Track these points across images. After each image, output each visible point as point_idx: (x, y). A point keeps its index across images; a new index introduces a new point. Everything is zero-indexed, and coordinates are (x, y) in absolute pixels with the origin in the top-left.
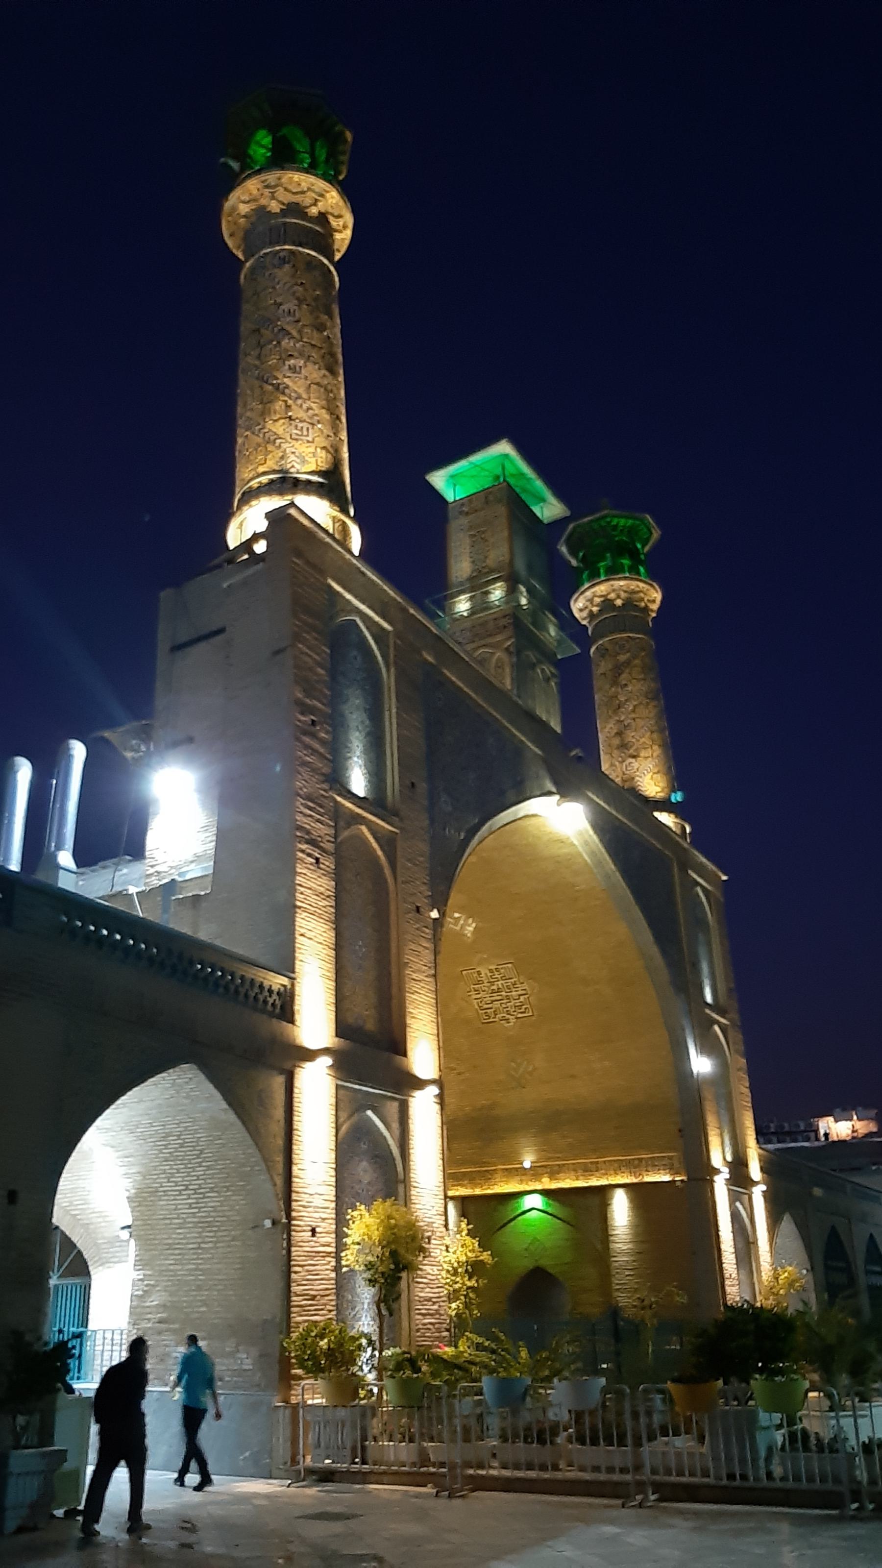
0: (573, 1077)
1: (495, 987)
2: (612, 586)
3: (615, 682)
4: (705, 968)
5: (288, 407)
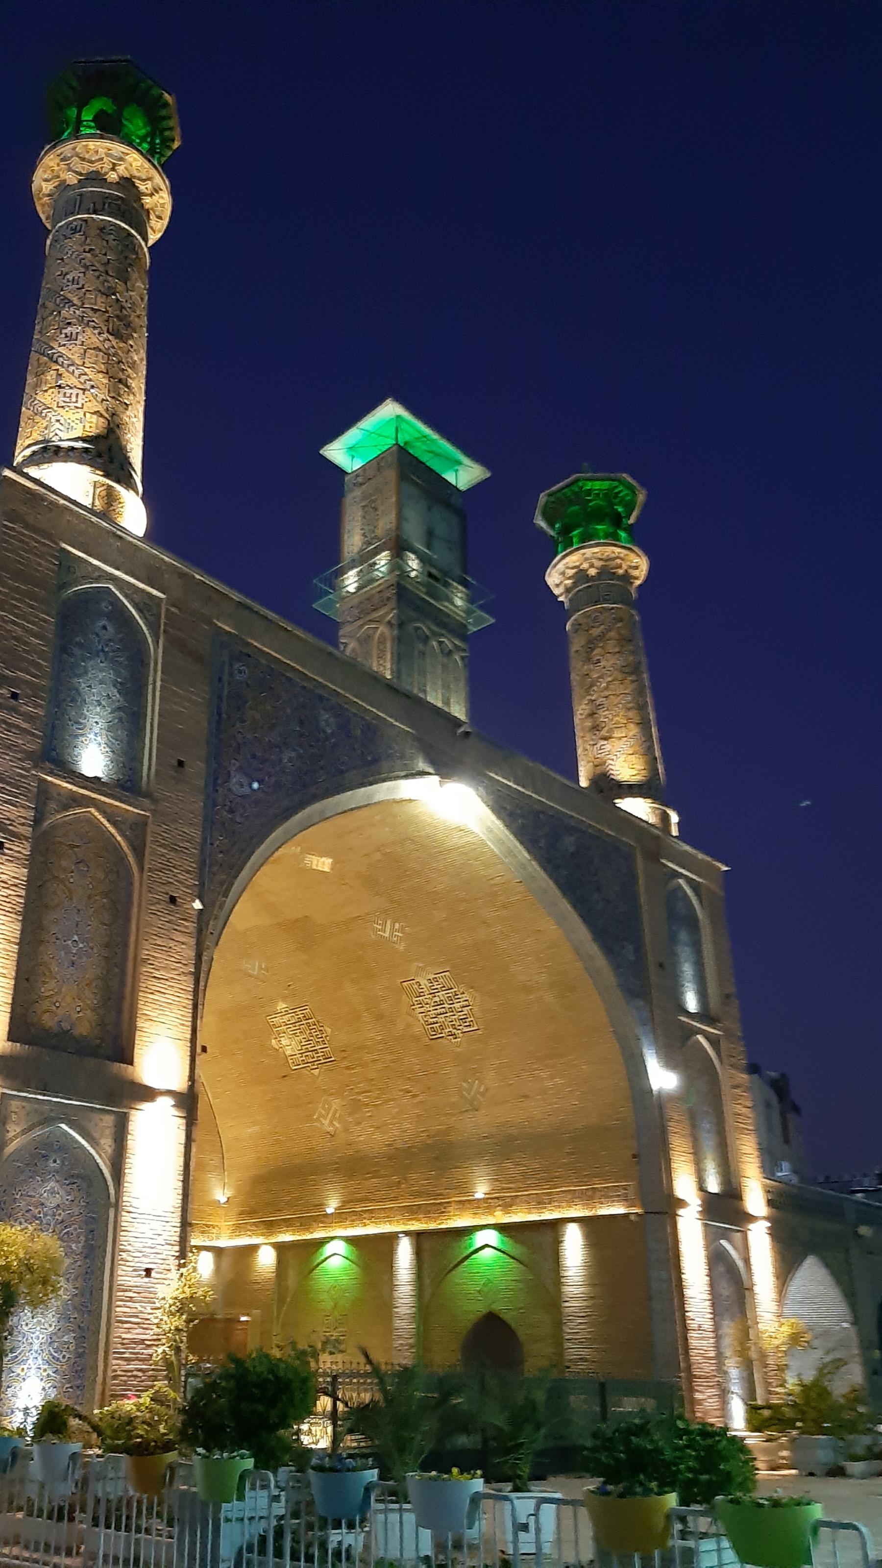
0: (526, 1096)
1: (437, 999)
2: (584, 554)
3: (588, 660)
4: (687, 970)
5: (60, 375)
